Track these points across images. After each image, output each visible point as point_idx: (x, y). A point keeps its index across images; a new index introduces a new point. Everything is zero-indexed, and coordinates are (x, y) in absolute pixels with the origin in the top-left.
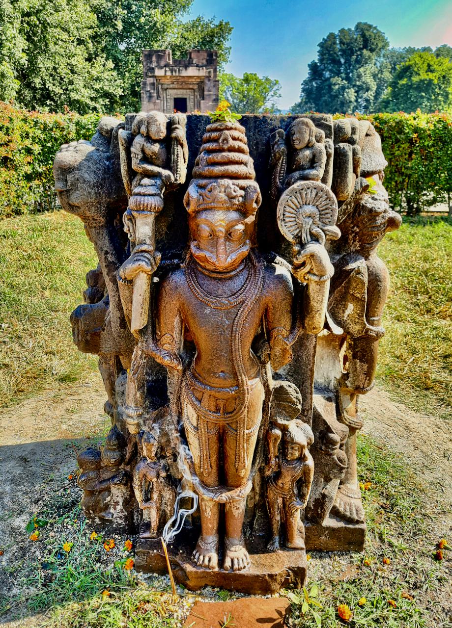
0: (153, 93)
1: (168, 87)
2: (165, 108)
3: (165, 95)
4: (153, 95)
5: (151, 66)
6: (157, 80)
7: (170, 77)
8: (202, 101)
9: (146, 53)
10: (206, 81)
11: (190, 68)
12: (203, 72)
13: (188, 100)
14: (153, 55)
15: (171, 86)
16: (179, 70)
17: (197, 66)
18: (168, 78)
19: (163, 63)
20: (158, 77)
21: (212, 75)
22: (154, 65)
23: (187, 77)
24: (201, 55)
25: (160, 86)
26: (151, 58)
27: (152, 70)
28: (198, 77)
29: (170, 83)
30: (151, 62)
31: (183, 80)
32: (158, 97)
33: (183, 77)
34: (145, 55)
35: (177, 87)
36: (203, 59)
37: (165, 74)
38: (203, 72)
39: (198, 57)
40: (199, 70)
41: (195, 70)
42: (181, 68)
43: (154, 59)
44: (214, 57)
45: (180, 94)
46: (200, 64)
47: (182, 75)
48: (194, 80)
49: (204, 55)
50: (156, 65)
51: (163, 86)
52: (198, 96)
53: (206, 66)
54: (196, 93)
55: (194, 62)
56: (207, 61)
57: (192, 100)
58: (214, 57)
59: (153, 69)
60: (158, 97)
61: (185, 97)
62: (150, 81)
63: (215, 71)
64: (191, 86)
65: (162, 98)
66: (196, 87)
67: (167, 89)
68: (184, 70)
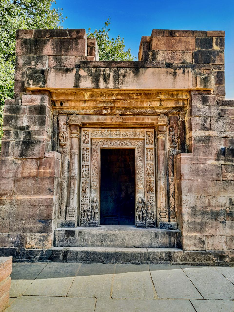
0: (38, 133)
1: (86, 121)
2: (75, 173)
3: (75, 141)
4: (36, 137)
5: (39, 67)
6: (53, 103)
7: (92, 96)
8: (184, 156)
9: (28, 37)
10: (197, 103)
11: (150, 70)
12: (185, 81)
13: (138, 155)
14: (45, 43)
15: (94, 119)
16: (117, 76)
17: (168, 66)
18: (86, 96)
19: (71, 60)
20: (58, 93)
21: (212, 85)
22: (47, 62)
23: (139, 93)
24: (180, 41)
25: (63, 119)
26: (42, 50)
27: (40, 76)
28: (170, 93)
29: (91, 111)
30: (40, 58)
31: (126, 103)
32: (57, 144)
33: (128, 95)
34: (25, 42)
35: (109, 122)
36: (183, 52)
37: (76, 86)
38: (185, 81)
39: (170, 46)
40: (175, 74)
41: (162, 76)
42: (122, 71)
43: (48, 49)
44: (216, 47)
45: (117, 139)
46: (176, 63)
47: (124, 87)
48: (157, 104)
49: (187, 43)
50: (53, 63)
51: (72, 118)
52: (168, 145)
53: (193, 67)
54: (161, 138)
55: (159, 58)
56: (195, 55)
57: (150, 154)
58: (216, 47)
59: (43, 72)
60: (57, 144)
61: (131, 146)
62: (32, 101)
63: (220, 79)
64: (148, 120)
65: (67, 149)
66: (162, 121)
67: (84, 126)
68: (132, 74)
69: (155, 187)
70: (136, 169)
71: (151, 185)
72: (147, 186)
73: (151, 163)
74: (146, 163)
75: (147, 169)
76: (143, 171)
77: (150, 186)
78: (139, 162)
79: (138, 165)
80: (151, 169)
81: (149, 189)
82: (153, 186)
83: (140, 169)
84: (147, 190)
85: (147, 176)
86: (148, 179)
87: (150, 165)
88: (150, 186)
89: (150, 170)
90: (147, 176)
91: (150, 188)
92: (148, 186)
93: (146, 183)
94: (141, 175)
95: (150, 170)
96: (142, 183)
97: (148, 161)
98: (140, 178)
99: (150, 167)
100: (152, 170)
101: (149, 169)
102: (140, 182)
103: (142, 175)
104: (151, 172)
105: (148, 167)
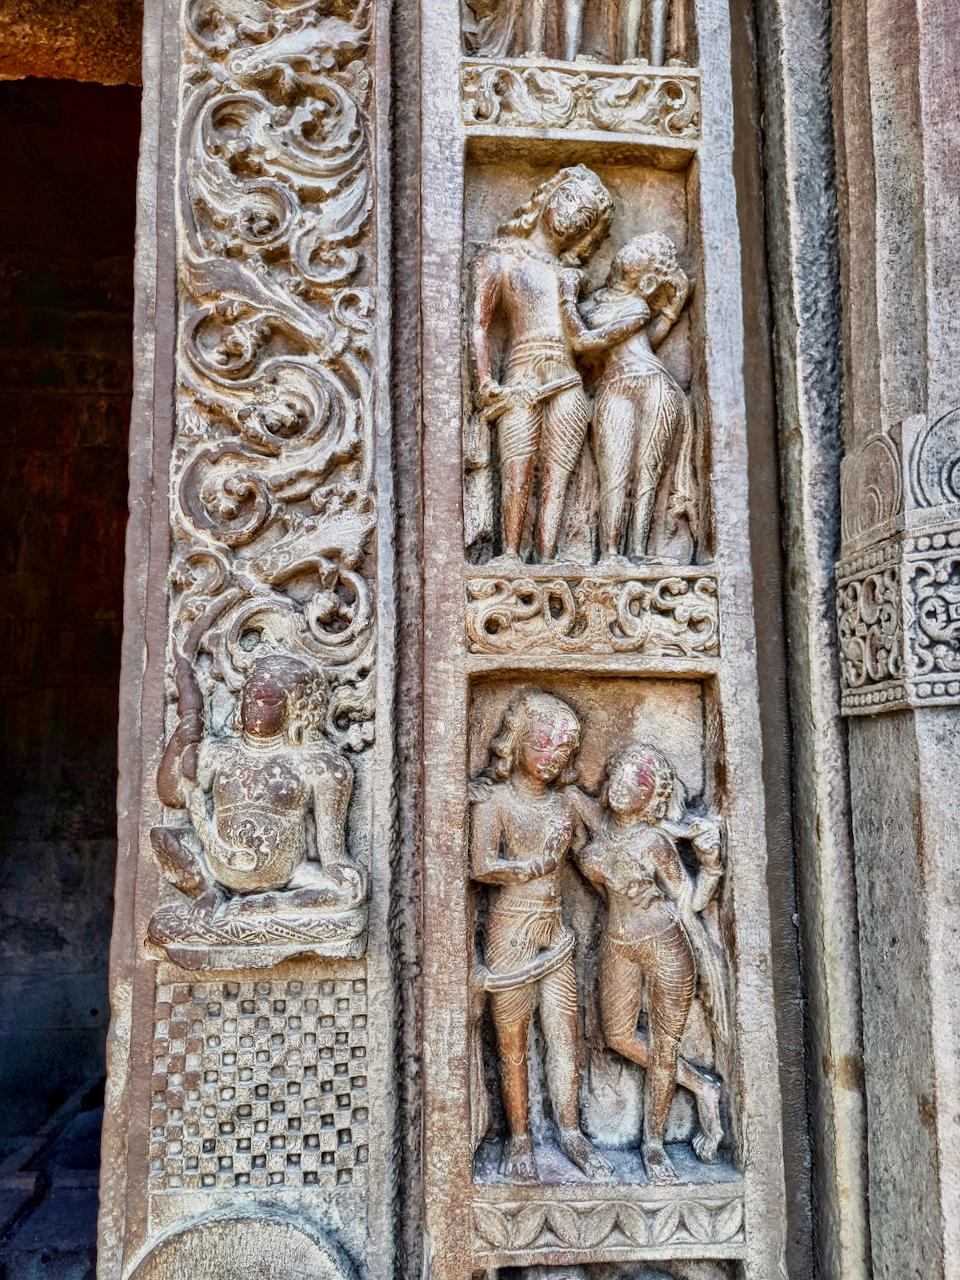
69: (755, 935)
70: (145, 349)
71: (627, 855)
72: (484, 893)
73: (634, 126)
74: (447, 118)
75: (502, 318)
76: (367, 419)
77: (576, 877)
78: (257, 130)
79: (201, 215)
80: (620, 309)
81: (557, 1002)
82: (689, 894)
83: (275, 336)
84: (486, 1027)
85: (489, 544)
86: (538, 644)
87: (579, 192)
88: (576, 877)
89: (592, 367)
90: (489, 544)
91: (592, 962)
92: (523, 914)
93: (445, 786)
94: (304, 546)
95: (592, 367)
96: (319, 781)
97: (533, 60)
98: (280, 626)
99: (587, 242)
100: (637, 355)
101: (545, 323)
102: (259, 751)
103: (342, 531)
104: (616, 412)
105: (539, 273)
